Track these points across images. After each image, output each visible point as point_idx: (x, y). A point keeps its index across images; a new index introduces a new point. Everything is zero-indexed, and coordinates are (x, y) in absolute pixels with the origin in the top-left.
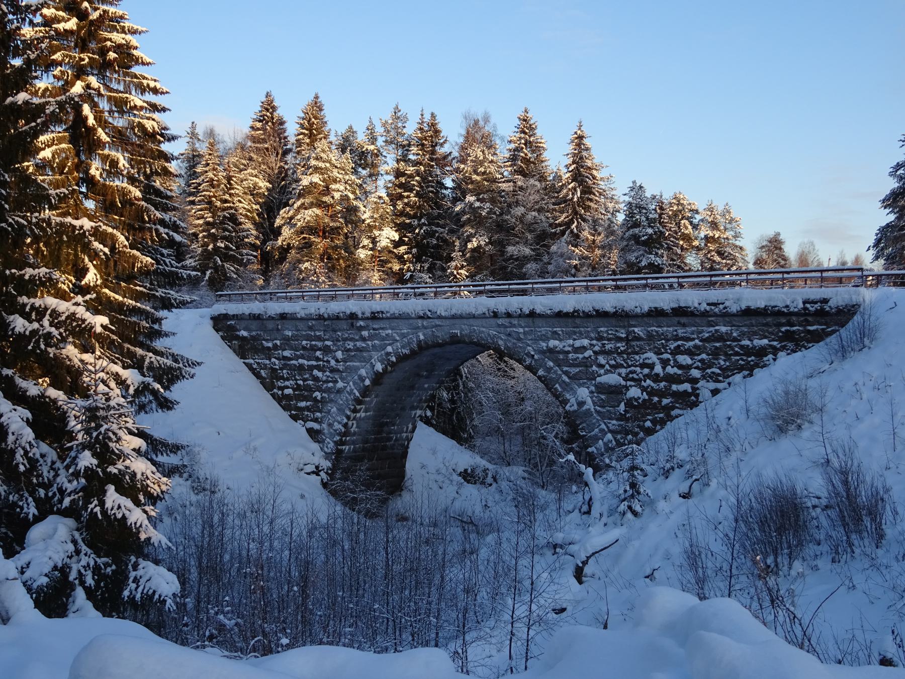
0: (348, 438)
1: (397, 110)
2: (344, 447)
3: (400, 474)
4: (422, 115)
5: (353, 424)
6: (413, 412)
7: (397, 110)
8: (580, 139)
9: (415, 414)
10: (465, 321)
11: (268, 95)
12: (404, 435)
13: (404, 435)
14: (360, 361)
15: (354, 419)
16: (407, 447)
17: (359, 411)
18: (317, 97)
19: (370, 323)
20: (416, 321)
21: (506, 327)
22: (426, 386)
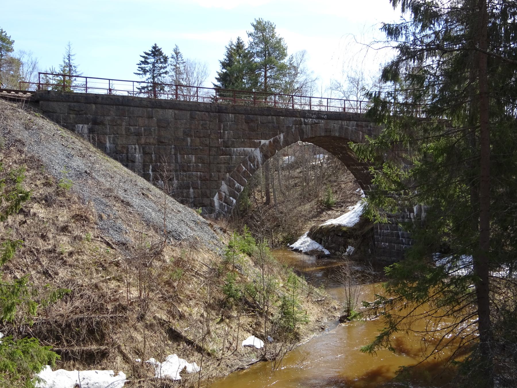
10: (336, 122)
14: (250, 147)
19: (259, 118)
20: (299, 119)
21: (362, 127)
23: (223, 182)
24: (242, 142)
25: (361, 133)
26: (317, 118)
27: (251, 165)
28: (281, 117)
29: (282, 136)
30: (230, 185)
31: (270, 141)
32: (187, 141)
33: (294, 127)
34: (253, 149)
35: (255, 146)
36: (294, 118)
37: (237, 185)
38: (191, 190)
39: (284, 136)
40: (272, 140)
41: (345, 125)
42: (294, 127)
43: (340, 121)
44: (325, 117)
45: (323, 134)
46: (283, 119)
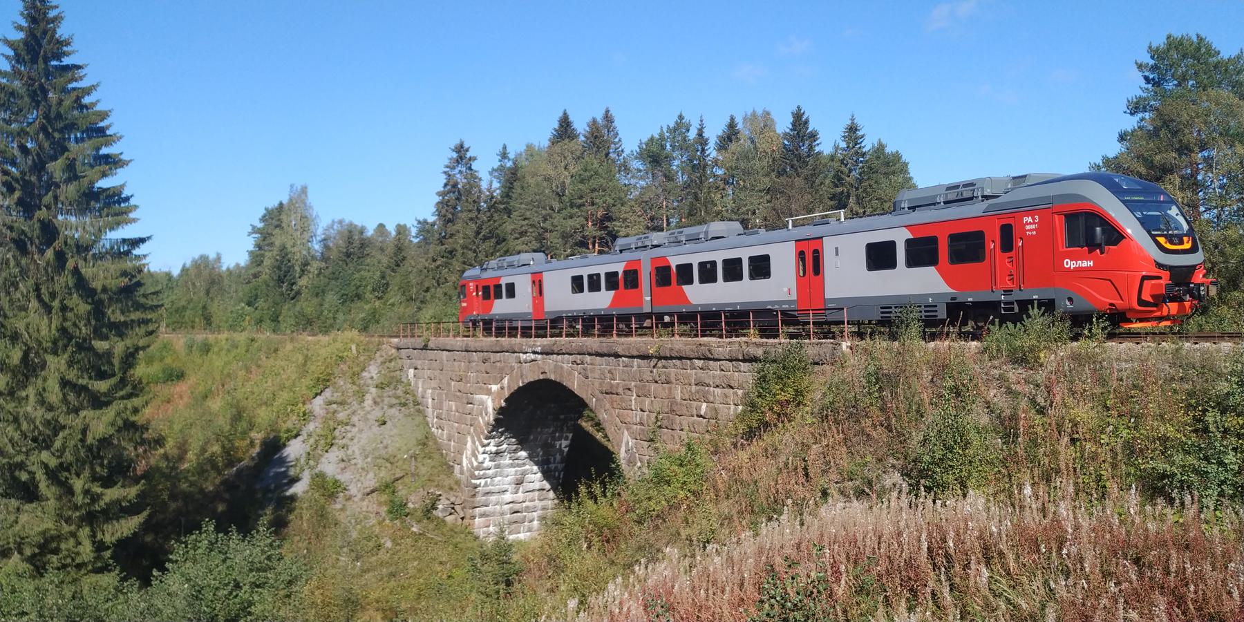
0: (482, 473)
1: (681, 117)
2: (477, 482)
4: (701, 121)
5: (485, 459)
6: (558, 444)
7: (681, 117)
9: (560, 445)
11: (565, 114)
12: (552, 466)
13: (552, 466)
15: (484, 453)
17: (488, 444)
18: (607, 111)
19: (492, 355)
22: (562, 417)
23: (469, 439)
24: (481, 388)
26: (534, 353)
29: (506, 381)
30: (474, 443)
32: (450, 385)
34: (487, 397)
35: (489, 392)
37: (477, 443)
38: (452, 443)
40: (499, 386)
43: (555, 356)
45: (542, 377)
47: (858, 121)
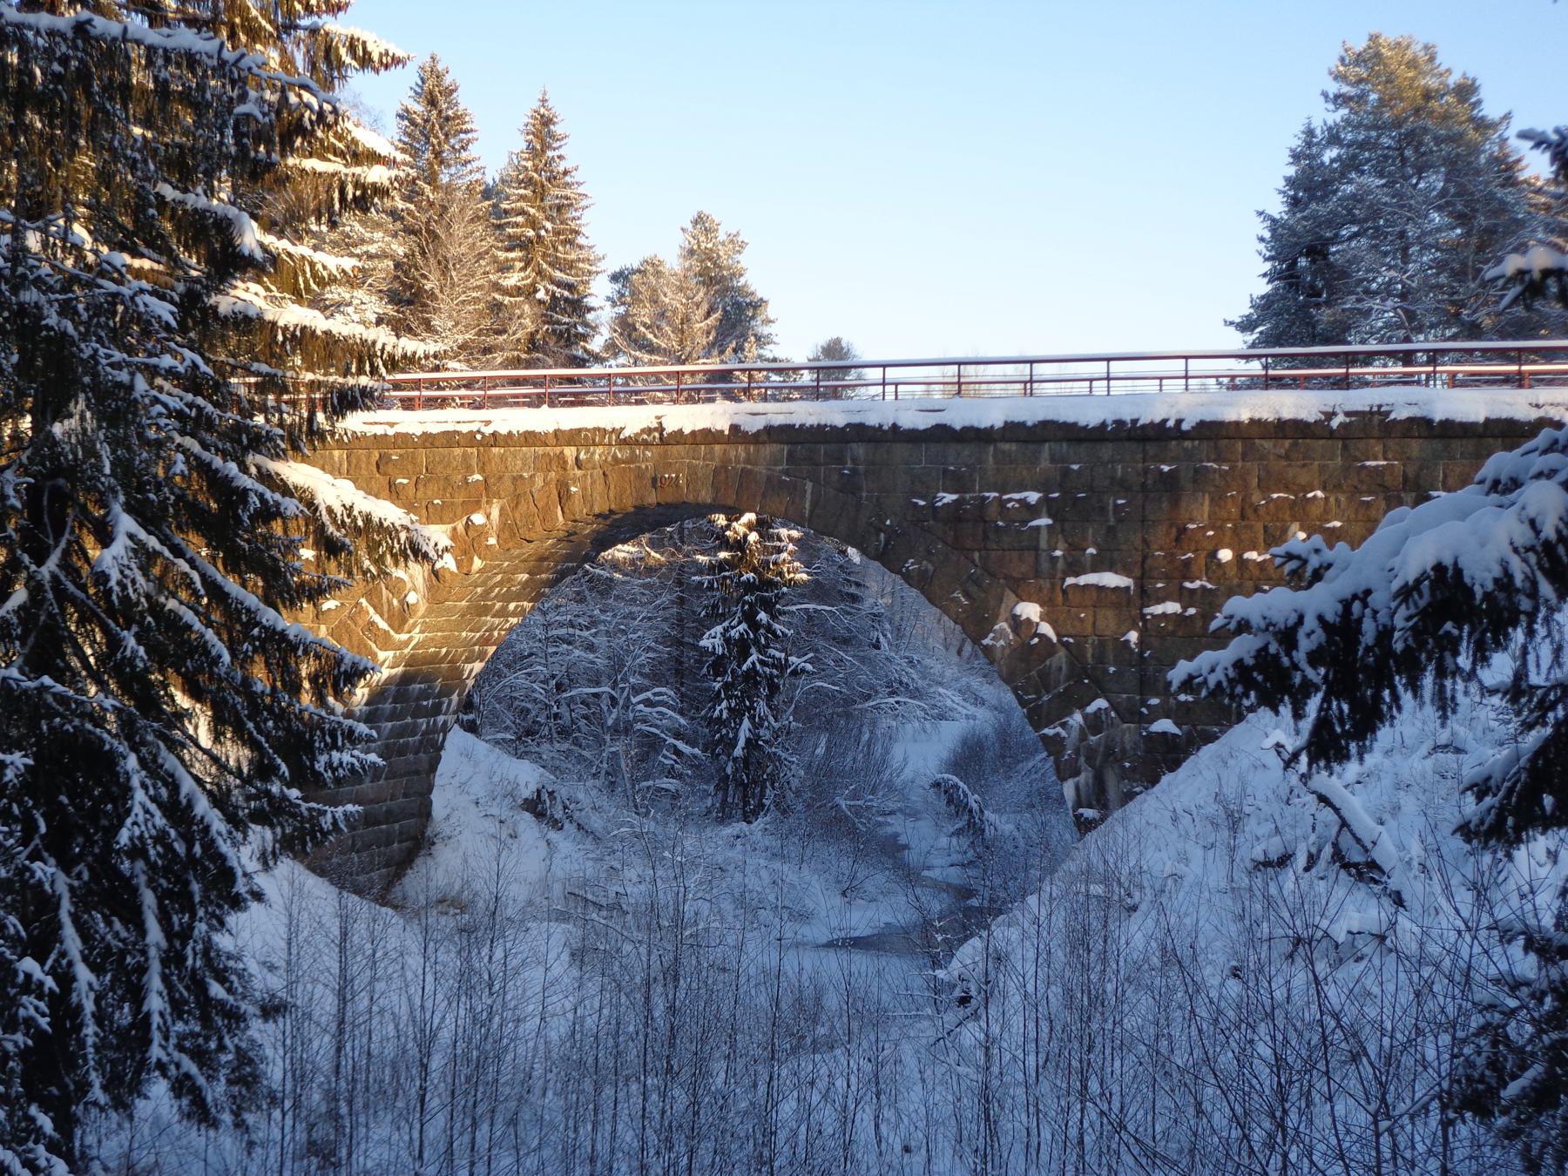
3: (425, 812)
6: (468, 667)
8: (543, 130)
13: (441, 719)
16: (442, 747)
20: (557, 450)
22: (512, 606)
25: (809, 486)
27: (395, 602)
28: (495, 450)
29: (495, 513)
31: (455, 529)
33: (539, 482)
36: (540, 450)
39: (502, 509)
41: (738, 462)
42: (539, 482)
43: (717, 448)
44: (650, 439)
45: (652, 498)
46: (502, 457)
47: (557, 106)
